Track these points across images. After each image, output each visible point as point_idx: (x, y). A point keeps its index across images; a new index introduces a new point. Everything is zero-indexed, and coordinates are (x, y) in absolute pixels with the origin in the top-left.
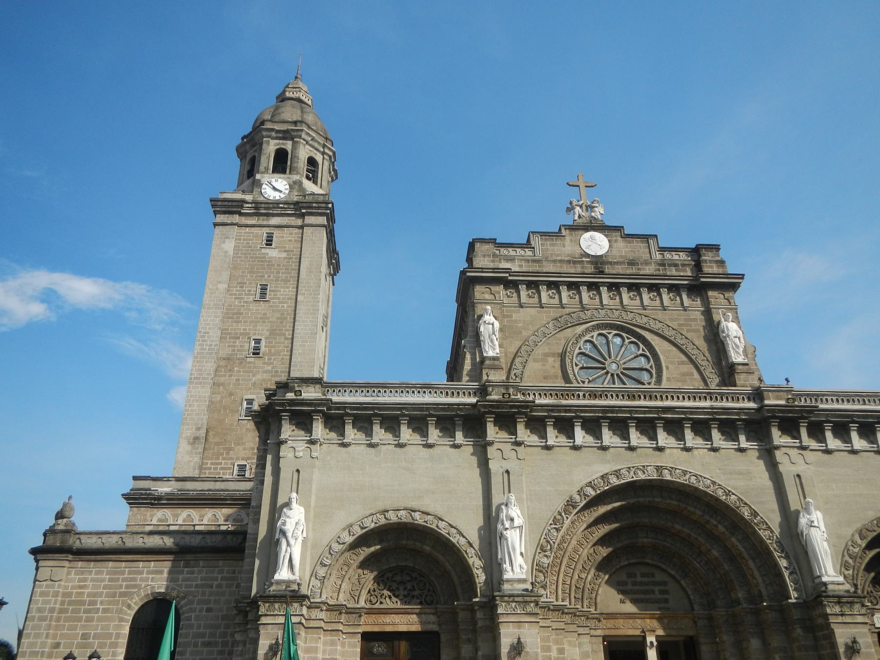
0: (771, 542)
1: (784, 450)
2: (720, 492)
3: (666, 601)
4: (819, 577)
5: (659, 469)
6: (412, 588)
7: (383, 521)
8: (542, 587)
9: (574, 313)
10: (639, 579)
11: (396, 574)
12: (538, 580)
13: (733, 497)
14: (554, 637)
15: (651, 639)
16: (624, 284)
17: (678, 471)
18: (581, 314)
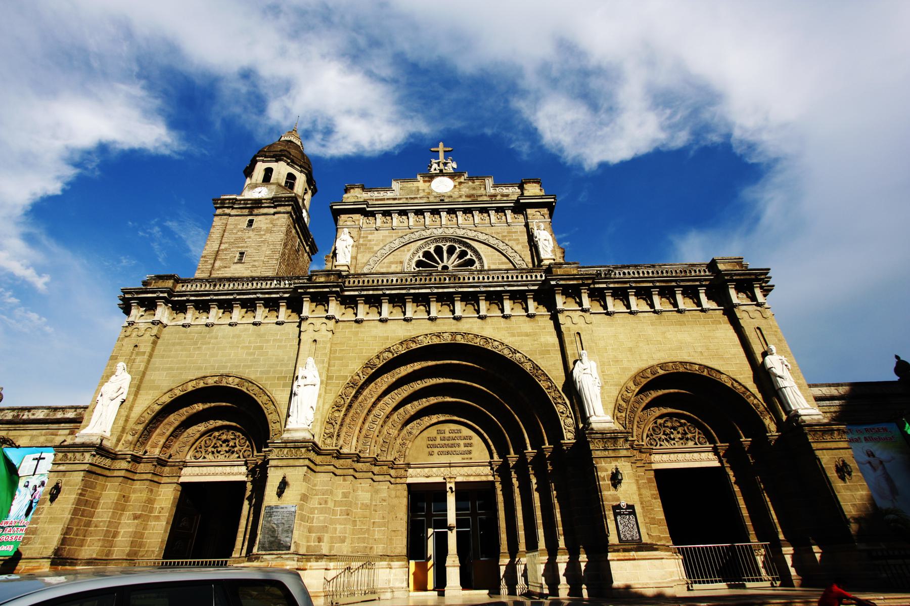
0: (549, 391)
1: (567, 313)
2: (506, 352)
3: (470, 452)
4: (589, 418)
5: (454, 334)
6: (233, 445)
7: (201, 385)
8: (330, 437)
9: (417, 232)
10: (447, 435)
11: (223, 433)
12: (327, 431)
13: (518, 354)
14: (342, 482)
15: (451, 485)
16: (459, 209)
17: (470, 335)
18: (424, 233)
